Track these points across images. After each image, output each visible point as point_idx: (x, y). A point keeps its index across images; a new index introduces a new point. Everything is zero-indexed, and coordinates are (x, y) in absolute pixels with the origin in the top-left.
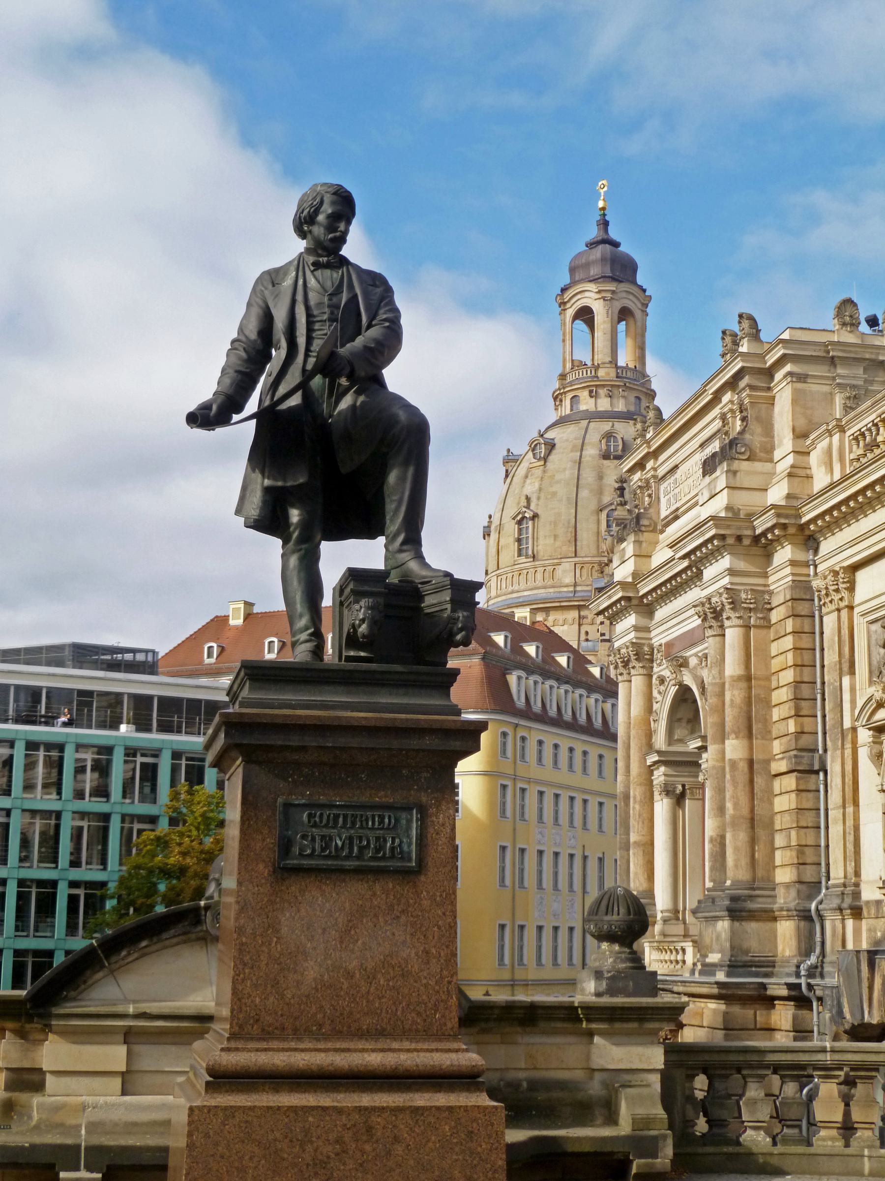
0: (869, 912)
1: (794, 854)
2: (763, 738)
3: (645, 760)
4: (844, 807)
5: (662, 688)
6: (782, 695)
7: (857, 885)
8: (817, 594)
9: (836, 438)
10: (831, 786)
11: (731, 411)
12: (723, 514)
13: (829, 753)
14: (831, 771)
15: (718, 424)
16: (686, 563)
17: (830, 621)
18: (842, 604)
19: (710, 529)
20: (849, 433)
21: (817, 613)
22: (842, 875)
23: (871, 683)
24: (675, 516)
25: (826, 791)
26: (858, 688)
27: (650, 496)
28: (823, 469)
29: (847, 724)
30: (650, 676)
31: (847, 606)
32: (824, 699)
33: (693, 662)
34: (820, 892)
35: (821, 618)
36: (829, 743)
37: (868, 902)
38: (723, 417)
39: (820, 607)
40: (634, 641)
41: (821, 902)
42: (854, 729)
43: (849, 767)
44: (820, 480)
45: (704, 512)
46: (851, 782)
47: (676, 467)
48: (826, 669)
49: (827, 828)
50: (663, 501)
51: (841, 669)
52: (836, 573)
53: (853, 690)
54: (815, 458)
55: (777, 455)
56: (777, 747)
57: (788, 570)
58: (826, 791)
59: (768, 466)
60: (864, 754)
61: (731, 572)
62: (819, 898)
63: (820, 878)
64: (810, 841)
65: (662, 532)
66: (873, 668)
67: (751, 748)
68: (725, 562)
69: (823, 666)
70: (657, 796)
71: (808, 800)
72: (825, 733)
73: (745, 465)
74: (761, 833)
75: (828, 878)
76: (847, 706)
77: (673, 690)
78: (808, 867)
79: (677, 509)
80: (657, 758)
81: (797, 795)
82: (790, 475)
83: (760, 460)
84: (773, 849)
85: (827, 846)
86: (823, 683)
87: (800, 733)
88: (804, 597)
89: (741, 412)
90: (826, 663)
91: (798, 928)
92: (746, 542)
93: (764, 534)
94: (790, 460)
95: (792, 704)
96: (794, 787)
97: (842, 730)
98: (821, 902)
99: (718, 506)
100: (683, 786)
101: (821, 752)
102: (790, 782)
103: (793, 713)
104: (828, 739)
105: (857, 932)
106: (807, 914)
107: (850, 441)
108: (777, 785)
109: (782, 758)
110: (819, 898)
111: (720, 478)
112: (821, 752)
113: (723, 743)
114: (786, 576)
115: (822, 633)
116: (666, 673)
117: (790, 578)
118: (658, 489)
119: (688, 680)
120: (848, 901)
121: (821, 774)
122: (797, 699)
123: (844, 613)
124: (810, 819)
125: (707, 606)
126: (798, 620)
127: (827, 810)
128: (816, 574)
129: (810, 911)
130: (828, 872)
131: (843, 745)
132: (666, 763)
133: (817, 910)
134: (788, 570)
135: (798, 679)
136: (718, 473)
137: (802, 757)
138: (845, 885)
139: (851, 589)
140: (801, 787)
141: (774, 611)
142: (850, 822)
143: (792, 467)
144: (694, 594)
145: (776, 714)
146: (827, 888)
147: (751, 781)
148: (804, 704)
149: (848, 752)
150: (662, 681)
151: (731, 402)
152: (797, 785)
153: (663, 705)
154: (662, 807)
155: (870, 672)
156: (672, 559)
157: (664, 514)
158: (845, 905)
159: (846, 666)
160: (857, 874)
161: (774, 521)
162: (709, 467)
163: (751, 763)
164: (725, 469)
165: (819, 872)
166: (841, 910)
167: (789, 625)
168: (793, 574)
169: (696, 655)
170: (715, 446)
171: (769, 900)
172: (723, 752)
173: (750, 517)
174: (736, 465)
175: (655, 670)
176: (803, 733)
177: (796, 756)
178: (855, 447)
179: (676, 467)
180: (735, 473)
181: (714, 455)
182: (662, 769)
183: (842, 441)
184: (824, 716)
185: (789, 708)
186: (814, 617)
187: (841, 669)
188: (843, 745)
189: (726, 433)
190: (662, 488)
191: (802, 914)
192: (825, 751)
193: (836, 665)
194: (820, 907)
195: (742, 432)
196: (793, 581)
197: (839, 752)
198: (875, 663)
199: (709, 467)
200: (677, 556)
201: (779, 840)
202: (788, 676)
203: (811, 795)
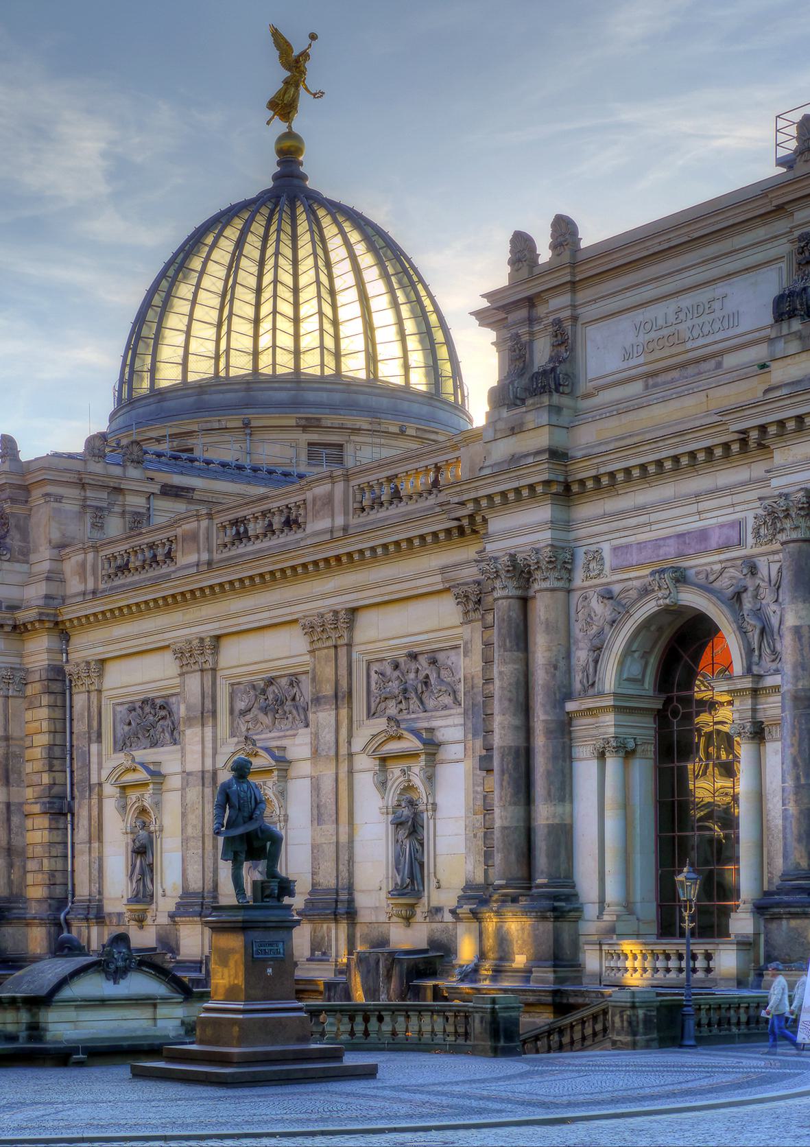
0: (111, 922)
1: (46, 876)
2: (18, 786)
4: (90, 843)
6: (37, 753)
7: (100, 901)
8: (68, 678)
9: (90, 556)
10: (78, 827)
13: (76, 801)
14: (79, 815)
17: (80, 701)
18: (93, 688)
20: (102, 554)
21: (68, 691)
22: (86, 892)
23: (115, 751)
25: (73, 829)
26: (104, 753)
28: (77, 578)
29: (94, 780)
31: (97, 690)
32: (72, 759)
34: (67, 906)
35: (71, 695)
36: (76, 793)
37: (110, 914)
39: (71, 687)
41: (68, 913)
42: (100, 785)
43: (95, 812)
44: (74, 586)
46: (96, 825)
48: (74, 736)
49: (73, 857)
51: (90, 738)
52: (88, 663)
53: (100, 754)
54: (69, 566)
55: (33, 558)
56: (29, 793)
57: (45, 656)
58: (73, 829)
60: (110, 807)
62: (67, 910)
63: (67, 896)
64: (60, 866)
66: (117, 739)
67: (9, 794)
69: (72, 733)
71: (58, 836)
72: (72, 785)
74: (17, 862)
75: (73, 896)
76: (94, 767)
78: (57, 887)
81: (50, 832)
82: (48, 579)
83: (18, 561)
84: (25, 872)
85: (73, 871)
86: (72, 746)
87: (53, 785)
88: (58, 678)
90: (75, 730)
91: (49, 933)
95: (46, 761)
96: (47, 825)
97: (90, 785)
98: (68, 913)
101: (69, 799)
102: (44, 822)
103: (47, 768)
104: (76, 790)
105: (100, 935)
106: (56, 921)
107: (102, 560)
108: (29, 823)
109: (37, 803)
110: (67, 910)
112: (69, 799)
114: (43, 660)
115: (71, 707)
117: (47, 662)
120: (93, 911)
121: (69, 815)
122: (51, 758)
123: (94, 696)
124: (59, 851)
126: (53, 697)
127: (73, 844)
128: (67, 661)
129: (60, 919)
130: (73, 890)
131: (90, 796)
133: (66, 919)
135: (52, 743)
137: (54, 803)
138: (90, 901)
139: (101, 675)
140: (52, 826)
141: (29, 686)
142: (95, 854)
143: (49, 572)
145: (29, 768)
146: (73, 903)
147: (9, 820)
148: (55, 762)
149: (95, 801)
152: (50, 824)
155: (115, 742)
158: (91, 916)
159: (94, 737)
160: (100, 893)
163: (8, 805)
165: (67, 890)
166: (87, 919)
167: (45, 700)
171: (22, 911)
176: (55, 784)
177: (49, 803)
178: (106, 566)
183: (95, 559)
184: (72, 772)
185: (44, 765)
186: (65, 694)
187: (90, 738)
188: (90, 796)
191: (53, 922)
192: (73, 798)
193: (85, 734)
194: (68, 917)
196: (49, 665)
197: (86, 801)
198: (119, 735)
201: (31, 865)
202: (44, 739)
203: (60, 832)
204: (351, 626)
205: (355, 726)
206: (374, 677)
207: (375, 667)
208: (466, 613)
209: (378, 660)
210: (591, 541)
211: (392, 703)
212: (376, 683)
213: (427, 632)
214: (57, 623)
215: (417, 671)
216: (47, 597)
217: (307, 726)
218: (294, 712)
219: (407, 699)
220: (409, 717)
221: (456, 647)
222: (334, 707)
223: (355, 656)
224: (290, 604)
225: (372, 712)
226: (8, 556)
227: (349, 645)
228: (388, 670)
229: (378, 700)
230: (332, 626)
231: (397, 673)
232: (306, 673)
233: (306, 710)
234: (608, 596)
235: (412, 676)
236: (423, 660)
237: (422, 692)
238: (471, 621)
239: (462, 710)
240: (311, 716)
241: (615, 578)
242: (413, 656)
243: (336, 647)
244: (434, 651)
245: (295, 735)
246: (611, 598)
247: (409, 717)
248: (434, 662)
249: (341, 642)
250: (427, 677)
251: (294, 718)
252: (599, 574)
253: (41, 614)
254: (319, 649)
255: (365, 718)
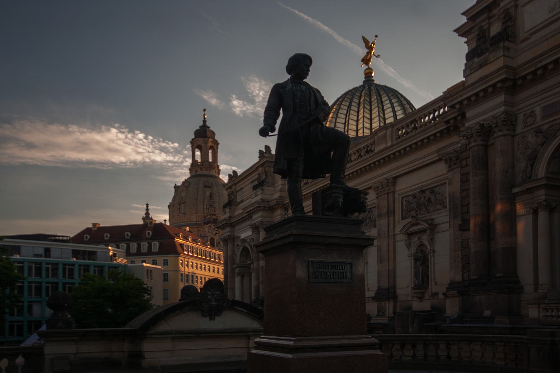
3: (232, 266)
5: (238, 248)
11: (262, 173)
12: (260, 201)
15: (257, 176)
16: (247, 214)
19: (256, 205)
24: (242, 202)
27: (233, 196)
30: (233, 244)
33: (248, 240)
38: (259, 174)
40: (229, 235)
45: (254, 200)
47: (242, 188)
50: (238, 197)
59: (273, 188)
61: (262, 216)
65: (237, 206)
68: (260, 214)
70: (236, 276)
73: (266, 188)
77: (241, 248)
79: (243, 200)
80: (236, 266)
82: (280, 191)
89: (265, 173)
92: (267, 208)
93: (272, 206)
94: (280, 187)
99: (258, 198)
100: (244, 273)
111: (259, 191)
113: (259, 262)
116: (239, 243)
118: (236, 195)
119: (247, 245)
125: (254, 226)
132: (239, 267)
134: (279, 216)
136: (258, 190)
144: (249, 222)
150: (238, 245)
151: (262, 170)
153: (238, 252)
154: (237, 279)
156: (243, 213)
157: (238, 201)
161: (276, 203)
162: (255, 188)
164: (261, 189)
168: (280, 217)
169: (249, 239)
170: (256, 183)
172: (259, 264)
173: (268, 202)
174: (264, 188)
175: (236, 243)
179: (242, 188)
180: (263, 190)
181: (256, 185)
182: (238, 269)
189: (260, 179)
190: (238, 194)
195: (265, 179)
199: (255, 188)
200: (245, 212)
204: (394, 184)
205: (396, 224)
206: (405, 203)
207: (404, 199)
208: (450, 167)
209: (406, 196)
210: (528, 108)
211: (414, 212)
212: (406, 206)
213: (430, 180)
214: (283, 205)
215: (425, 197)
216: (280, 197)
217: (375, 227)
218: (370, 223)
219: (420, 209)
220: (421, 216)
221: (445, 183)
222: (387, 217)
223: (396, 196)
224: (368, 181)
225: (404, 217)
226: (267, 185)
227: (394, 192)
228: (411, 199)
229: (407, 212)
230: (386, 185)
231: (415, 200)
232: (375, 207)
233: (375, 221)
234: (538, 131)
235: (422, 199)
236: (428, 193)
237: (427, 205)
238: (452, 170)
239: (448, 209)
240: (377, 223)
241: (543, 123)
242: (423, 192)
243: (388, 193)
244: (433, 188)
245: (370, 231)
246: (541, 132)
247: (421, 216)
248: (433, 192)
249: (389, 191)
250: (430, 198)
251: (370, 225)
252: (533, 123)
253: (277, 202)
254: (381, 196)
255: (401, 220)
